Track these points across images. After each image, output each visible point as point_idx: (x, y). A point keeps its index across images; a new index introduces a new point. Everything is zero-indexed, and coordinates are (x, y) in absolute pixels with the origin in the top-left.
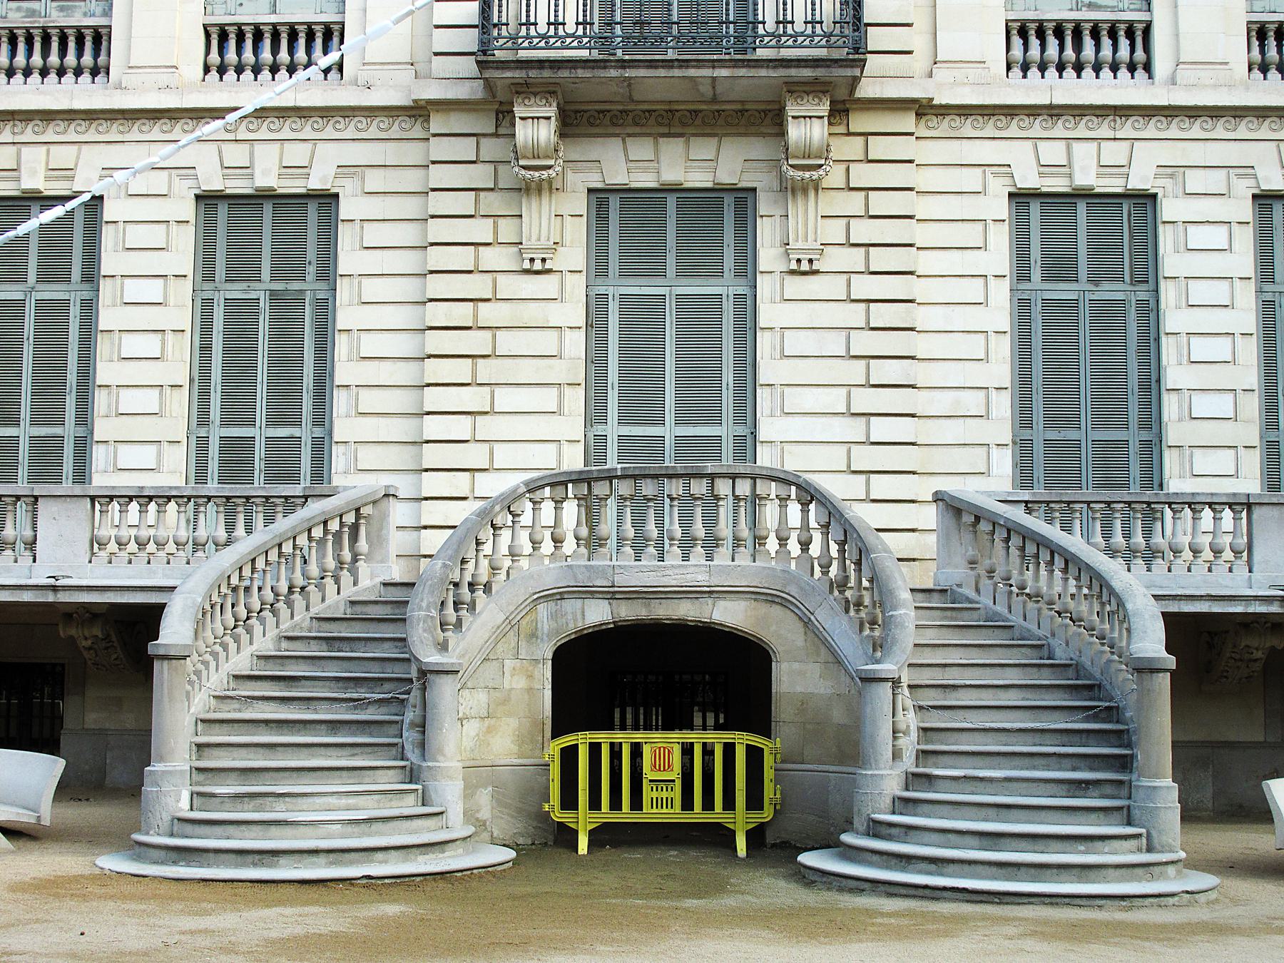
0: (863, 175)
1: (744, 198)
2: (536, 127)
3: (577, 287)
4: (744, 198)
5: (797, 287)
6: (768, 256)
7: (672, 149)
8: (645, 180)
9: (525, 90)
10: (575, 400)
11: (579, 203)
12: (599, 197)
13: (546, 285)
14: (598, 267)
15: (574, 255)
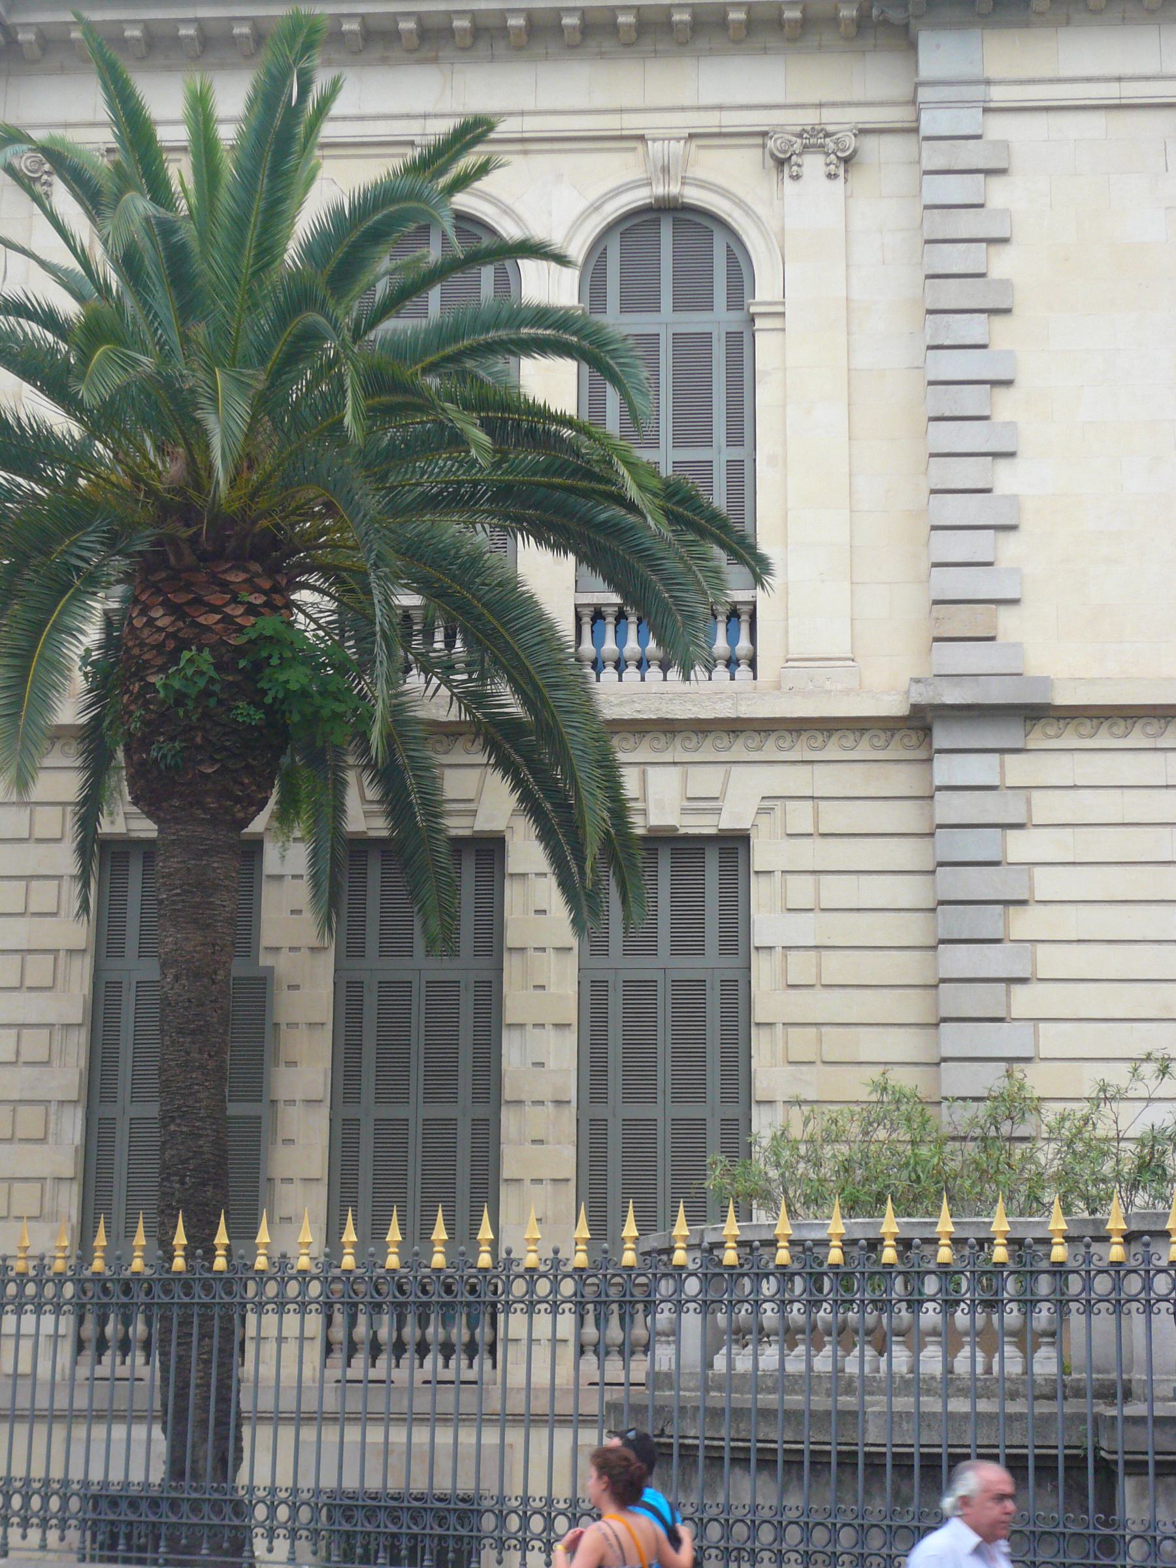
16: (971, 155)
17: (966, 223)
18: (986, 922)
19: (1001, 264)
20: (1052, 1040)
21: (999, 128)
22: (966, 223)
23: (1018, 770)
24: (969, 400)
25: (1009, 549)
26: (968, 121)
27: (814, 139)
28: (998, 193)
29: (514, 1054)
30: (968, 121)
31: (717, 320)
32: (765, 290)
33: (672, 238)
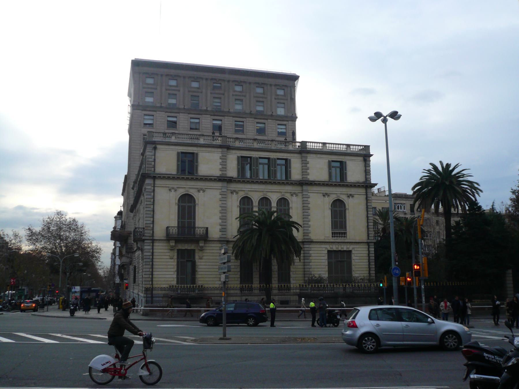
0: (207, 248)
1: (194, 250)
2: (172, 243)
3: (176, 260)
4: (194, 250)
5: (200, 261)
6: (197, 257)
7: (186, 245)
8: (184, 248)
9: (171, 240)
10: (176, 273)
11: (176, 251)
12: (178, 250)
13: (172, 260)
14: (178, 258)
15: (176, 257)
16: (307, 196)
17: (306, 202)
18: (308, 258)
19: (309, 206)
20: (313, 267)
21: (309, 194)
22: (306, 202)
23: (310, 246)
24: (307, 217)
25: (310, 229)
26: (307, 193)
27: (295, 193)
28: (309, 200)
29: (273, 268)
30: (307, 193)
31: (287, 208)
32: (290, 206)
33: (283, 202)
